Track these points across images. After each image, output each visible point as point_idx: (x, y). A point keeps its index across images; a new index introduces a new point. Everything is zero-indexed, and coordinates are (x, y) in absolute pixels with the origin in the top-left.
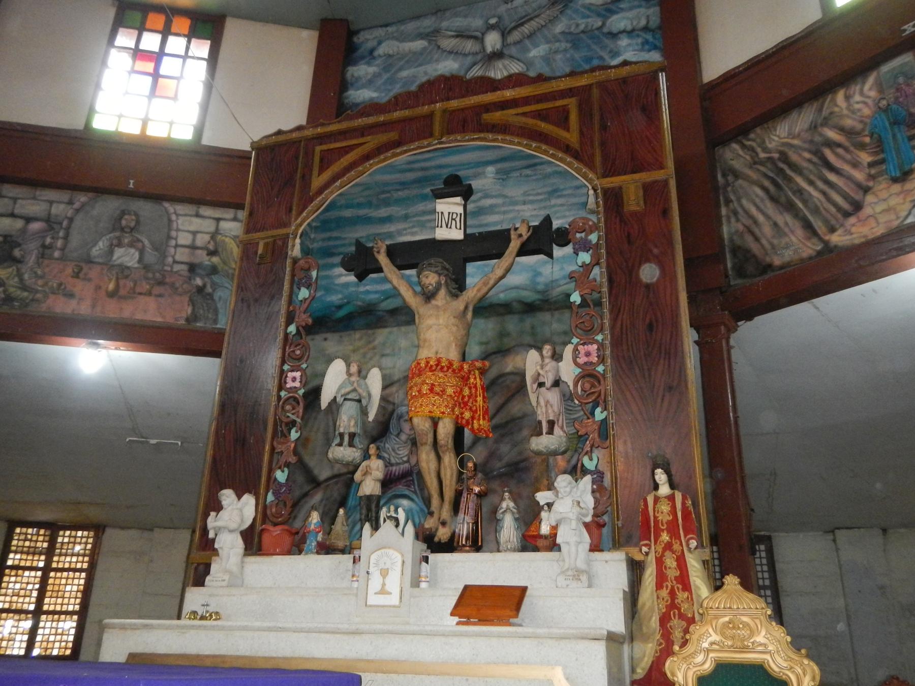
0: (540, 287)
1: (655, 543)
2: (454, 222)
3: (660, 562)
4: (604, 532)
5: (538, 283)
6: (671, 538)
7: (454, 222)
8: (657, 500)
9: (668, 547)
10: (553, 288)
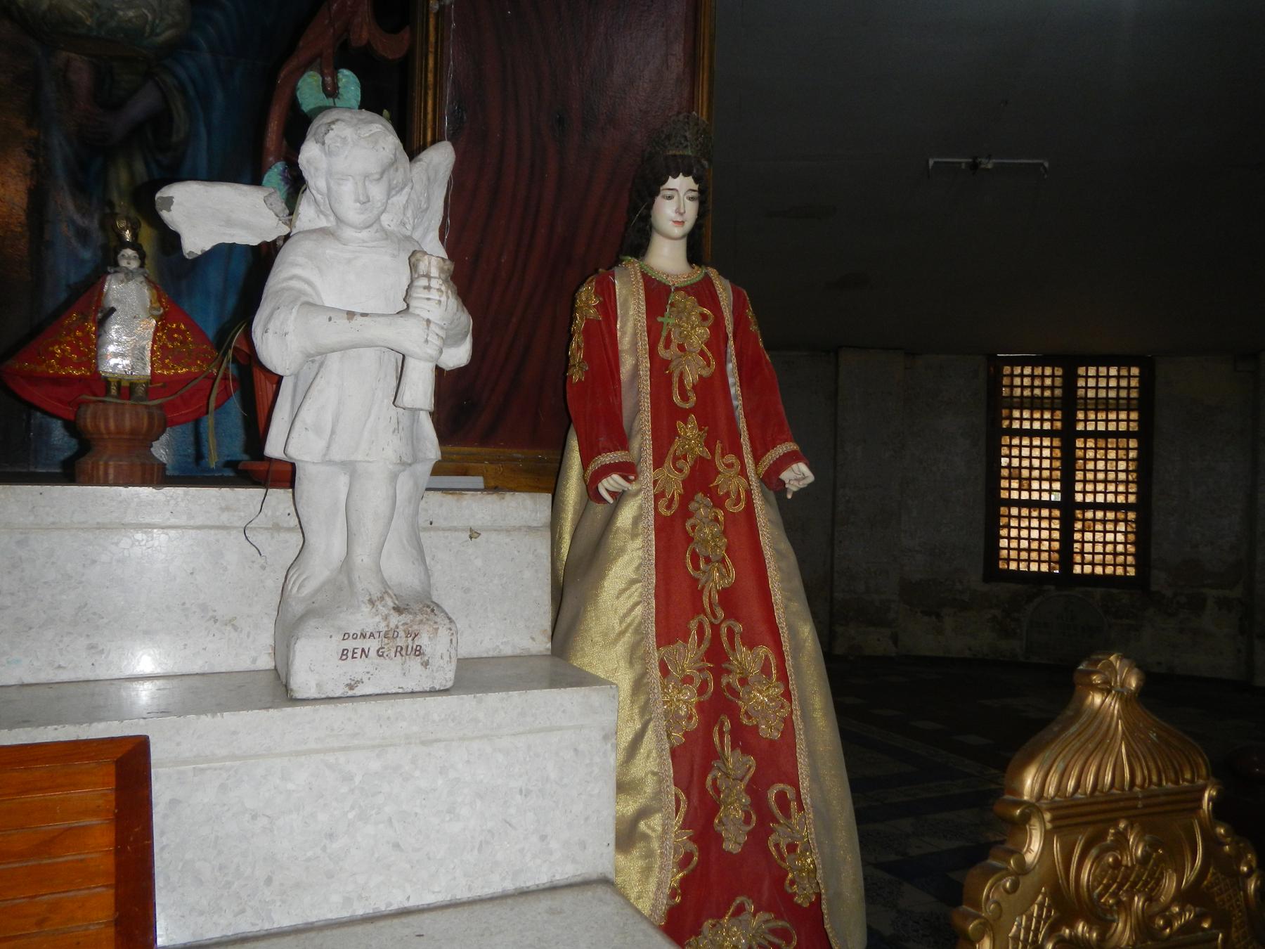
1: (658, 463)
3: (671, 535)
4: (509, 410)
6: (710, 444)
8: (657, 294)
9: (701, 479)
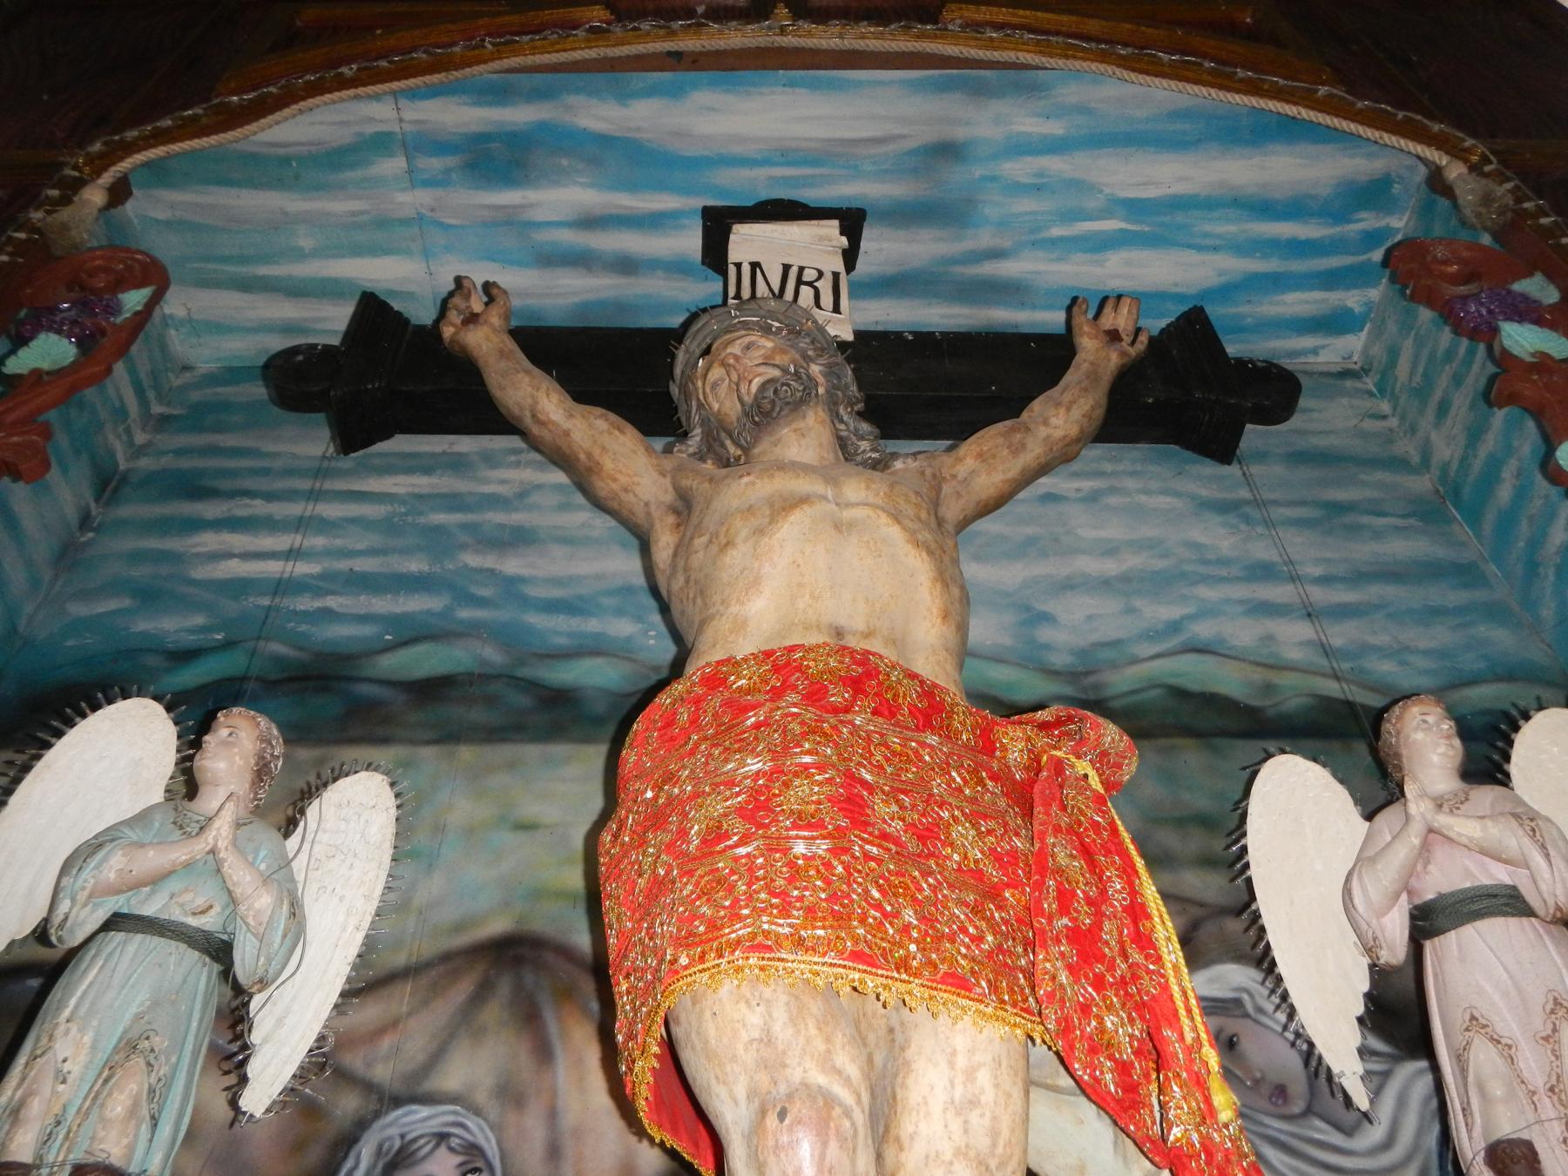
0: (1060, 660)
2: (806, 292)
5: (1047, 647)
7: (806, 292)
10: (1114, 665)
